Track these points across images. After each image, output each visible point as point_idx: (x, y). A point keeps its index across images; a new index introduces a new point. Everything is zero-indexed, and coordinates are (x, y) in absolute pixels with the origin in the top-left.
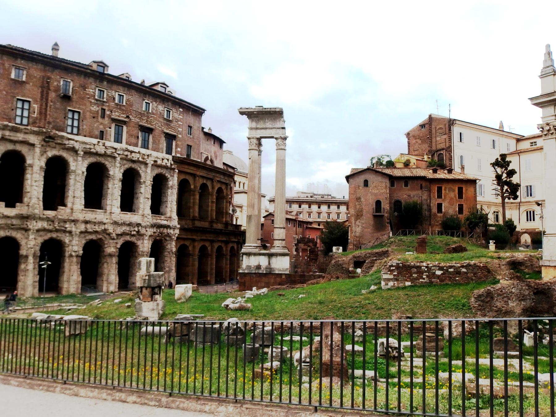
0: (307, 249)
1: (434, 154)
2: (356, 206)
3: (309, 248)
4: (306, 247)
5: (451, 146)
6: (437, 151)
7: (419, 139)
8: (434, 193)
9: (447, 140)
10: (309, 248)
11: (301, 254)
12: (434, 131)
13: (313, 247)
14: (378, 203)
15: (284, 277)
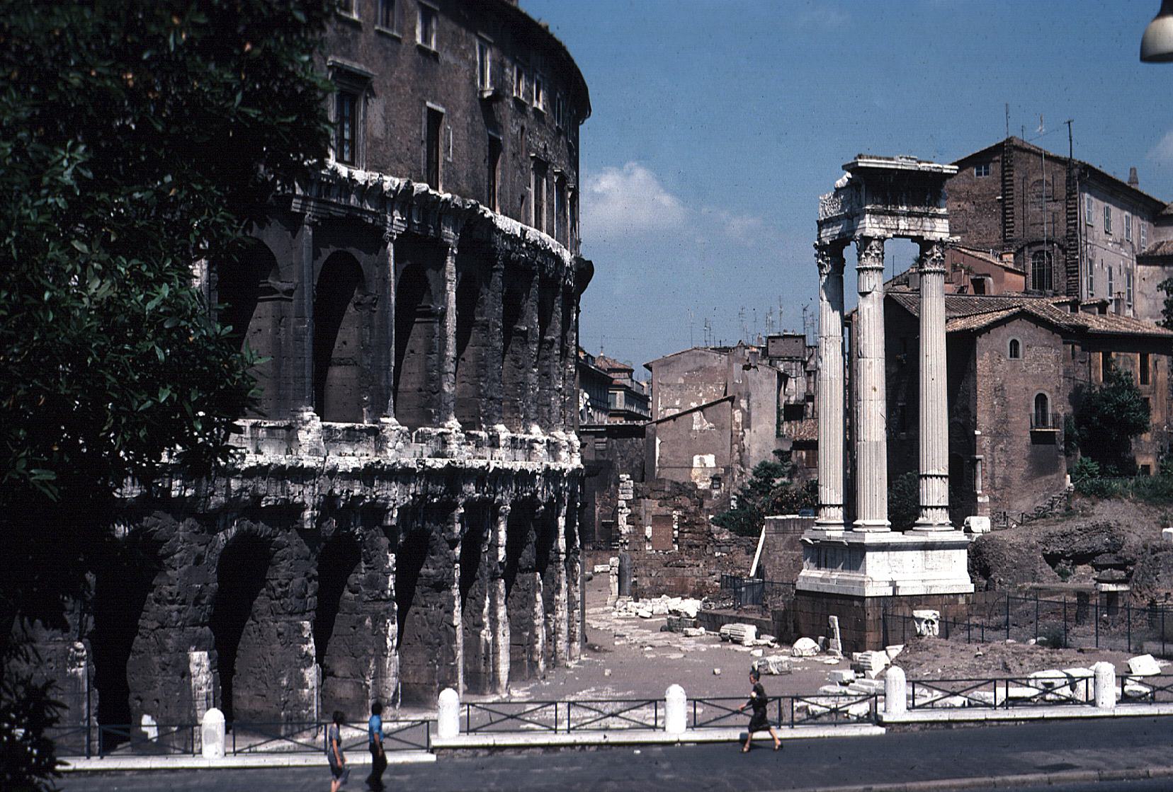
0: (670, 517)
1: (1022, 249)
2: (993, 406)
3: (676, 514)
4: (663, 511)
5: (1075, 235)
6: (1031, 245)
7: (967, 200)
8: (1096, 368)
9: (1062, 217)
10: (676, 514)
11: (649, 531)
12: (1018, 187)
13: (692, 509)
14: (1041, 400)
15: (962, 601)
